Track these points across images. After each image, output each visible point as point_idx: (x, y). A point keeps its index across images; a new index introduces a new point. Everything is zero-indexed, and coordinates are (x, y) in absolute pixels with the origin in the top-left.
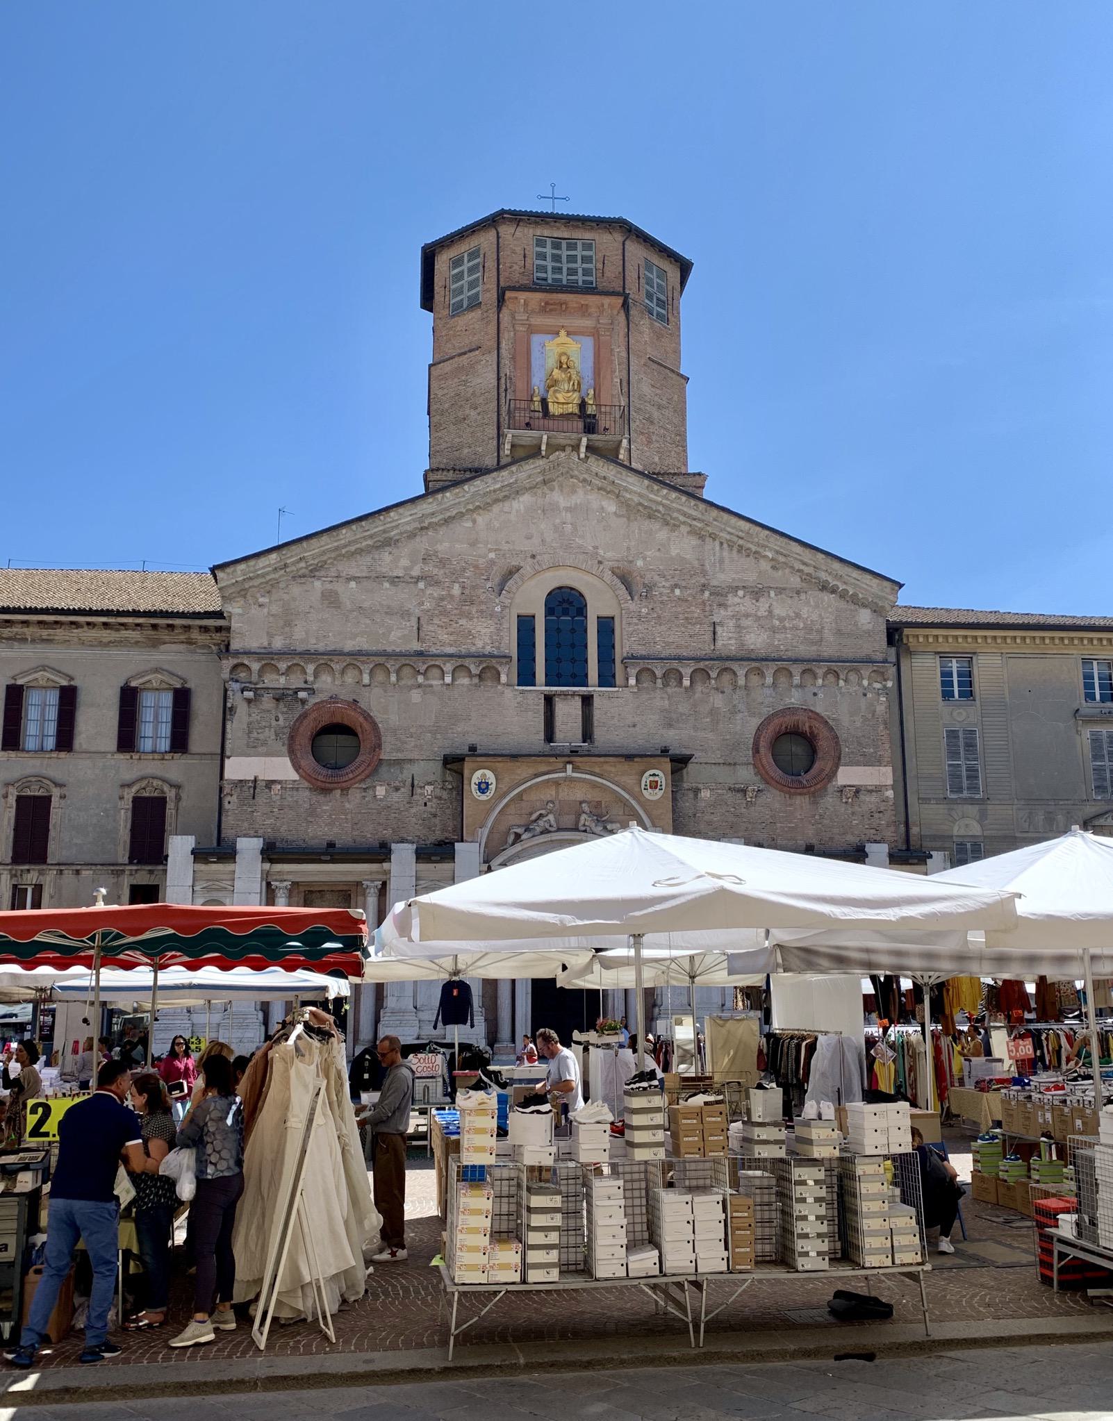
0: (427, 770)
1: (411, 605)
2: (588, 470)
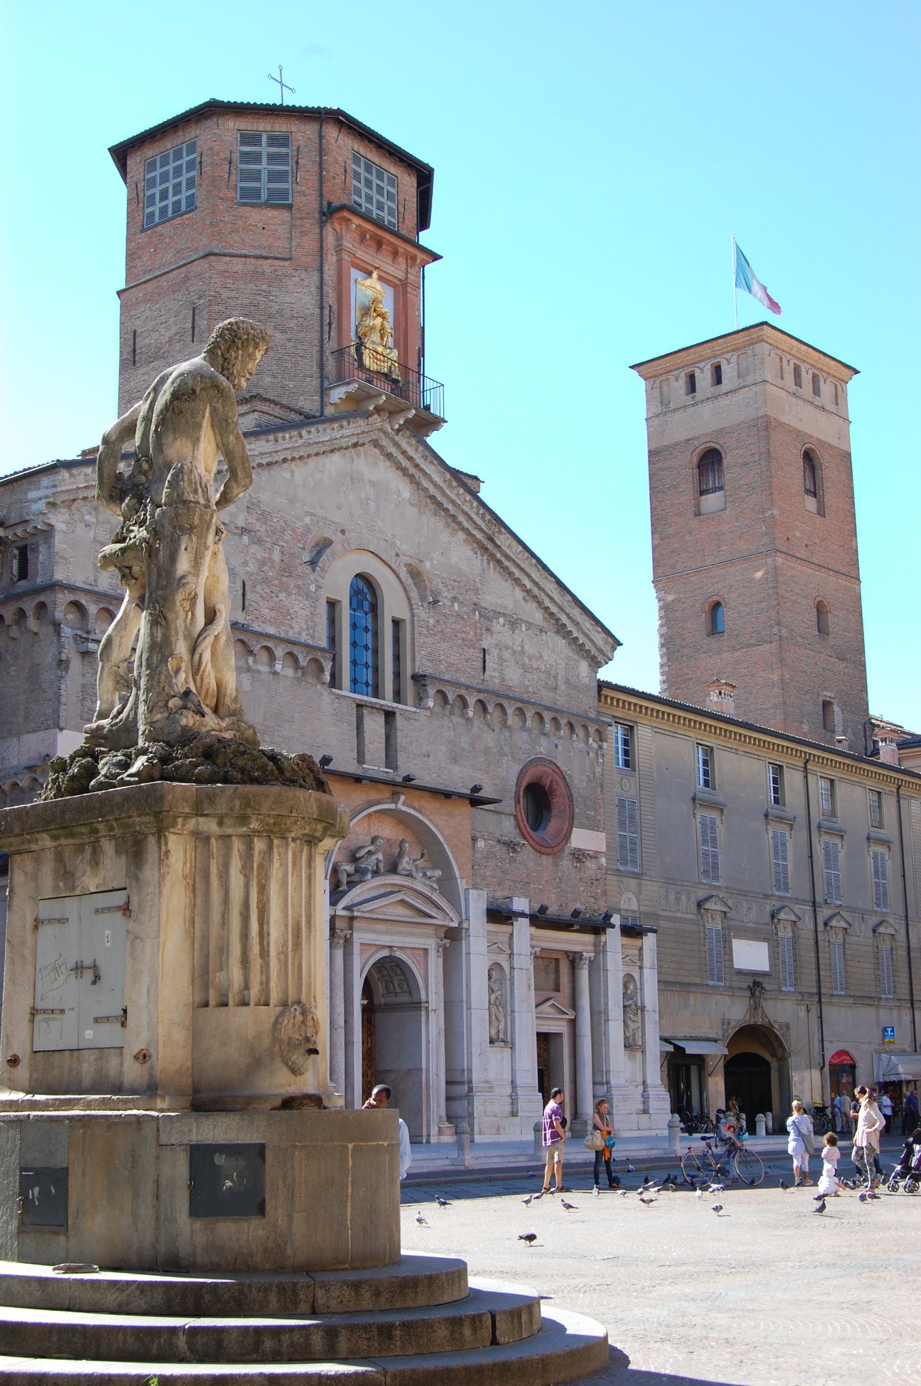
2: (397, 445)
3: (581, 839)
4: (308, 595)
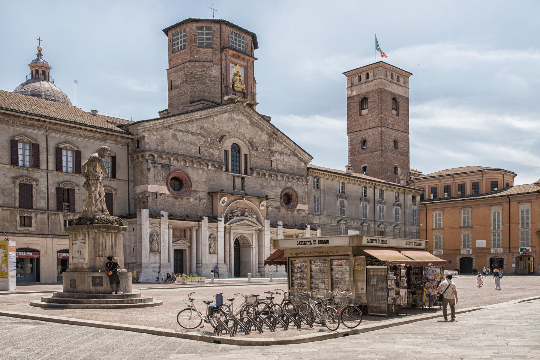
0: (203, 195)
1: (197, 142)
4: (218, 149)
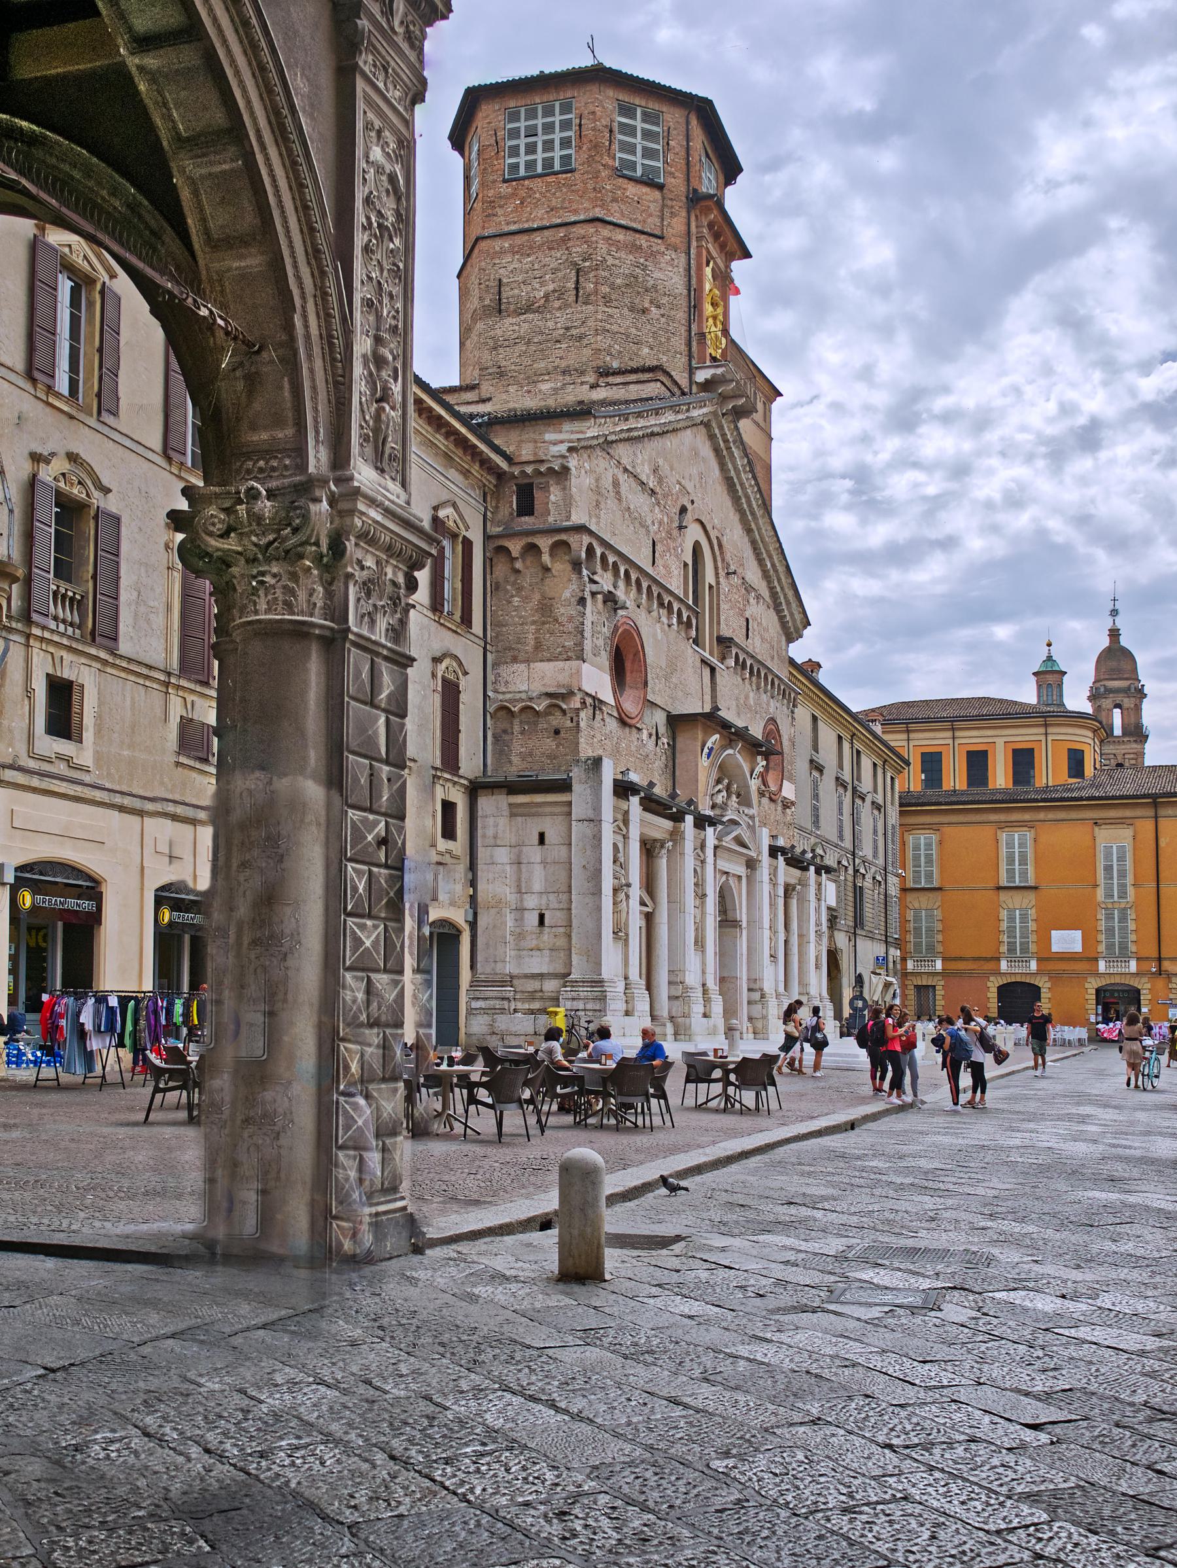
3: (788, 791)
